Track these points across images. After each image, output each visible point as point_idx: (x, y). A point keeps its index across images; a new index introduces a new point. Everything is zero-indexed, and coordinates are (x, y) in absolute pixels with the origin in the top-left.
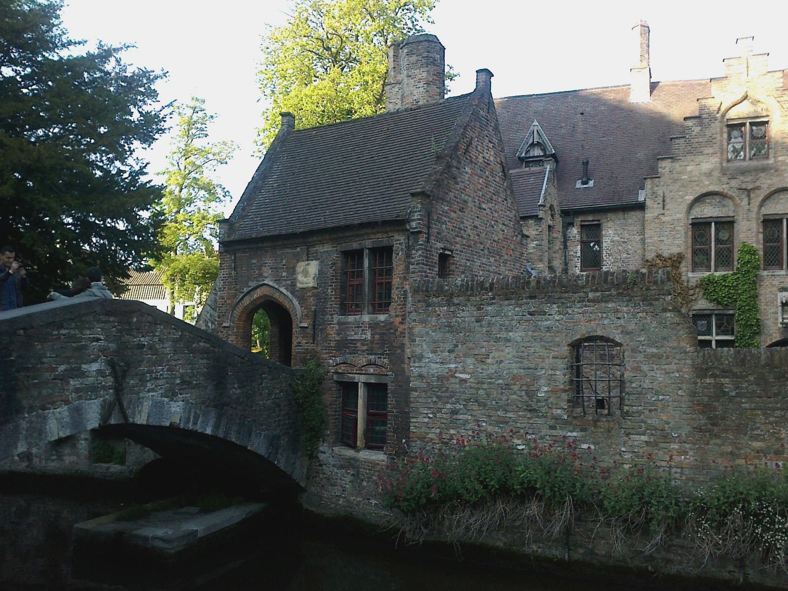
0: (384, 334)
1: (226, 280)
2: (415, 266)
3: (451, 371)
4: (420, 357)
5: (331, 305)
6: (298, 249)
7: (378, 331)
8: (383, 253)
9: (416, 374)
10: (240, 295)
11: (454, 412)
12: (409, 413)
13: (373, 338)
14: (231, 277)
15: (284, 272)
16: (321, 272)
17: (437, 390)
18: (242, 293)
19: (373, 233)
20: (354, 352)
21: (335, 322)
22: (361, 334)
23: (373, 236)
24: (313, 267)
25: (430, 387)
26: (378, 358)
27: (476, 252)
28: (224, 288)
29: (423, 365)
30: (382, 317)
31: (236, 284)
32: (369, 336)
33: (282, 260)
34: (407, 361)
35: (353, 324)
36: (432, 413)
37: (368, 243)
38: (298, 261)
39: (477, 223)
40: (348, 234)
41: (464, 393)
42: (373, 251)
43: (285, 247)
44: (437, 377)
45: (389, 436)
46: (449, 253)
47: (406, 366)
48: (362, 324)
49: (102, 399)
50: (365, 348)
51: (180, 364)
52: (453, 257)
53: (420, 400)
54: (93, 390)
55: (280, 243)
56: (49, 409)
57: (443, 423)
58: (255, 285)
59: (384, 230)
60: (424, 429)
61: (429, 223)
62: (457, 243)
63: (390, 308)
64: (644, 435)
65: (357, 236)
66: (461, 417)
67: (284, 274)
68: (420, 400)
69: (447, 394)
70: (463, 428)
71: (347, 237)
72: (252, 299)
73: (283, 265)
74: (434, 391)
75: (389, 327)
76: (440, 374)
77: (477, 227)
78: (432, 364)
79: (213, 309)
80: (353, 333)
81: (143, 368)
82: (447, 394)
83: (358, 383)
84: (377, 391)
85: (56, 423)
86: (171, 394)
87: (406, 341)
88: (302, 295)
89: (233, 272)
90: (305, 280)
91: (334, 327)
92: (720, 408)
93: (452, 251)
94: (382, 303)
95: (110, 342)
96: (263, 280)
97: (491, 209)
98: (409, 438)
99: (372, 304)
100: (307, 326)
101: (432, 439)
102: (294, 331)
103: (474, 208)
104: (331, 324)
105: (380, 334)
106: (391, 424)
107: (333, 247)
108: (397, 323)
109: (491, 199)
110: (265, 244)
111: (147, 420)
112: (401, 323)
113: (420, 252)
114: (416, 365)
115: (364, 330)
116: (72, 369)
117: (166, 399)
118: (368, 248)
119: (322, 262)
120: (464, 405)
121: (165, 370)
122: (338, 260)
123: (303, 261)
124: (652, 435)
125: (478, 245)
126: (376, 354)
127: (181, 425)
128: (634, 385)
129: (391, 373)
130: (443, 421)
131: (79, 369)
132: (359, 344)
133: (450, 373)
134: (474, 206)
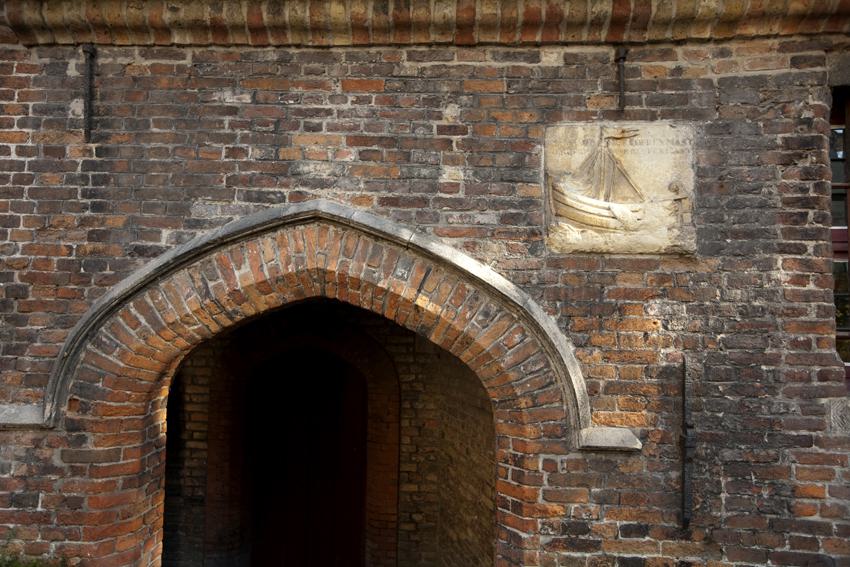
14: (60, 168)
15: (454, 161)
31: (96, 207)
33: (434, 102)
67: (450, 174)
88: (592, 291)
89: (76, 149)
90: (622, 209)
104: (808, 442)
123: (586, 117)
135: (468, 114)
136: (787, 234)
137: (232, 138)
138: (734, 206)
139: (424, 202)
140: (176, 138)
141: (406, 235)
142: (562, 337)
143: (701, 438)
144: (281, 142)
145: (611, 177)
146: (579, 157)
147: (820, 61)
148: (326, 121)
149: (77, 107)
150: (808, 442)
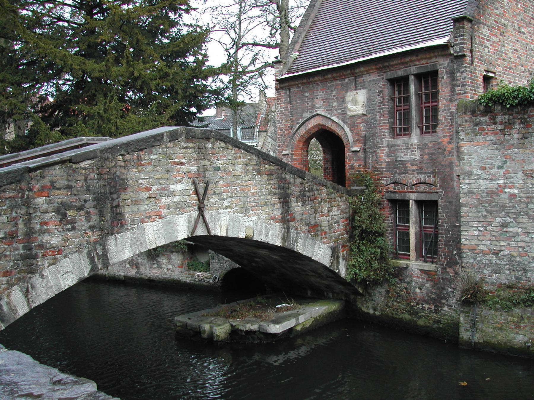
0: (432, 154)
1: (283, 113)
2: (460, 88)
3: (500, 186)
4: (470, 174)
5: (380, 130)
6: (347, 80)
7: (427, 151)
8: (429, 78)
9: (465, 191)
10: (295, 127)
11: (504, 225)
12: (460, 226)
13: (422, 158)
14: (288, 110)
16: (369, 100)
17: (486, 205)
18: (298, 123)
19: (418, 60)
20: (405, 172)
21: (385, 144)
22: (410, 155)
23: (417, 63)
24: (361, 96)
25: (481, 203)
26: (428, 177)
27: (518, 74)
28: (282, 121)
29: (471, 181)
30: (429, 138)
31: (292, 116)
32: (417, 156)
33: (332, 91)
34: (456, 179)
35: (403, 146)
36: (483, 226)
37: (414, 70)
38: (347, 91)
39: (518, 46)
40: (393, 63)
41: (513, 207)
42: (418, 76)
43: (334, 79)
44: (487, 193)
45: (440, 248)
46: (492, 75)
47: (455, 184)
48: (411, 145)
49: (188, 214)
50: (415, 168)
51: (251, 184)
52: (496, 79)
53: (470, 214)
54: (180, 208)
55: (329, 76)
56: (147, 222)
57: (494, 236)
58: (309, 116)
59: (428, 56)
60: (474, 242)
61: (472, 47)
62: (499, 65)
63: (437, 129)
65: (402, 64)
66: (511, 230)
67: (335, 104)
68: (470, 214)
69: (497, 209)
70: (513, 240)
71: (393, 66)
72: (307, 128)
73: (334, 96)
74: (484, 206)
75: (437, 147)
76: (489, 190)
77: (517, 51)
78: (481, 181)
79: (273, 139)
80: (402, 154)
81: (220, 188)
82: (497, 209)
83: (409, 201)
84: (428, 207)
85: (154, 235)
86: (245, 210)
87: (455, 159)
89: (289, 106)
90: (355, 107)
91: (384, 150)
93: (494, 73)
94: (430, 123)
95: (192, 166)
96: (316, 111)
97: (530, 33)
98: (460, 249)
99: (419, 127)
100: (358, 150)
101: (482, 251)
102: (347, 155)
103: (514, 32)
104: (381, 147)
105: (429, 154)
106: (442, 237)
107: (379, 76)
108: (445, 143)
109: (530, 23)
110: (316, 78)
111: (227, 233)
112: (450, 143)
113: (465, 74)
114: (467, 181)
115: (413, 151)
116: (163, 189)
117: (240, 215)
118: (414, 75)
119: (370, 90)
120: (514, 218)
121: (238, 189)
122: (384, 88)
123: (351, 91)
125: (520, 67)
126: (425, 173)
127: (255, 237)
129: (441, 190)
130: (495, 234)
131: (167, 189)
132: (408, 165)
133: (499, 189)
134: (514, 30)
135: (336, 93)
136: (379, 109)
137: (307, 102)
138: (372, 104)
139: (331, 110)
140: (301, 103)
141: (329, 116)
142: (349, 132)
143: (368, 148)
144: (313, 102)
145: (355, 102)
146: (351, 98)
147: (383, 75)
148: (318, 97)
149: (289, 99)
150: (381, 147)
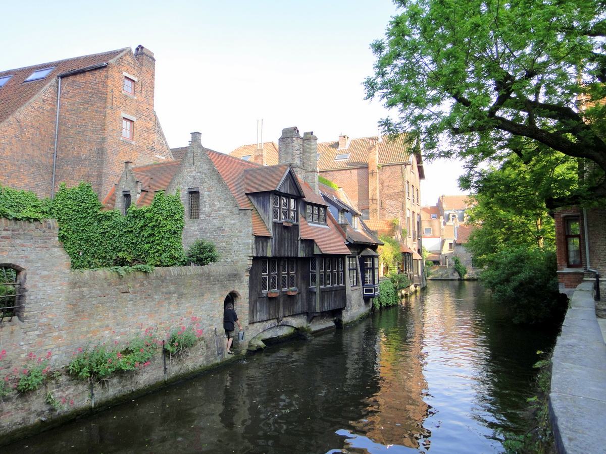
64: (37, 330)
92: (82, 305)
124: (42, 329)
128: (32, 297)
